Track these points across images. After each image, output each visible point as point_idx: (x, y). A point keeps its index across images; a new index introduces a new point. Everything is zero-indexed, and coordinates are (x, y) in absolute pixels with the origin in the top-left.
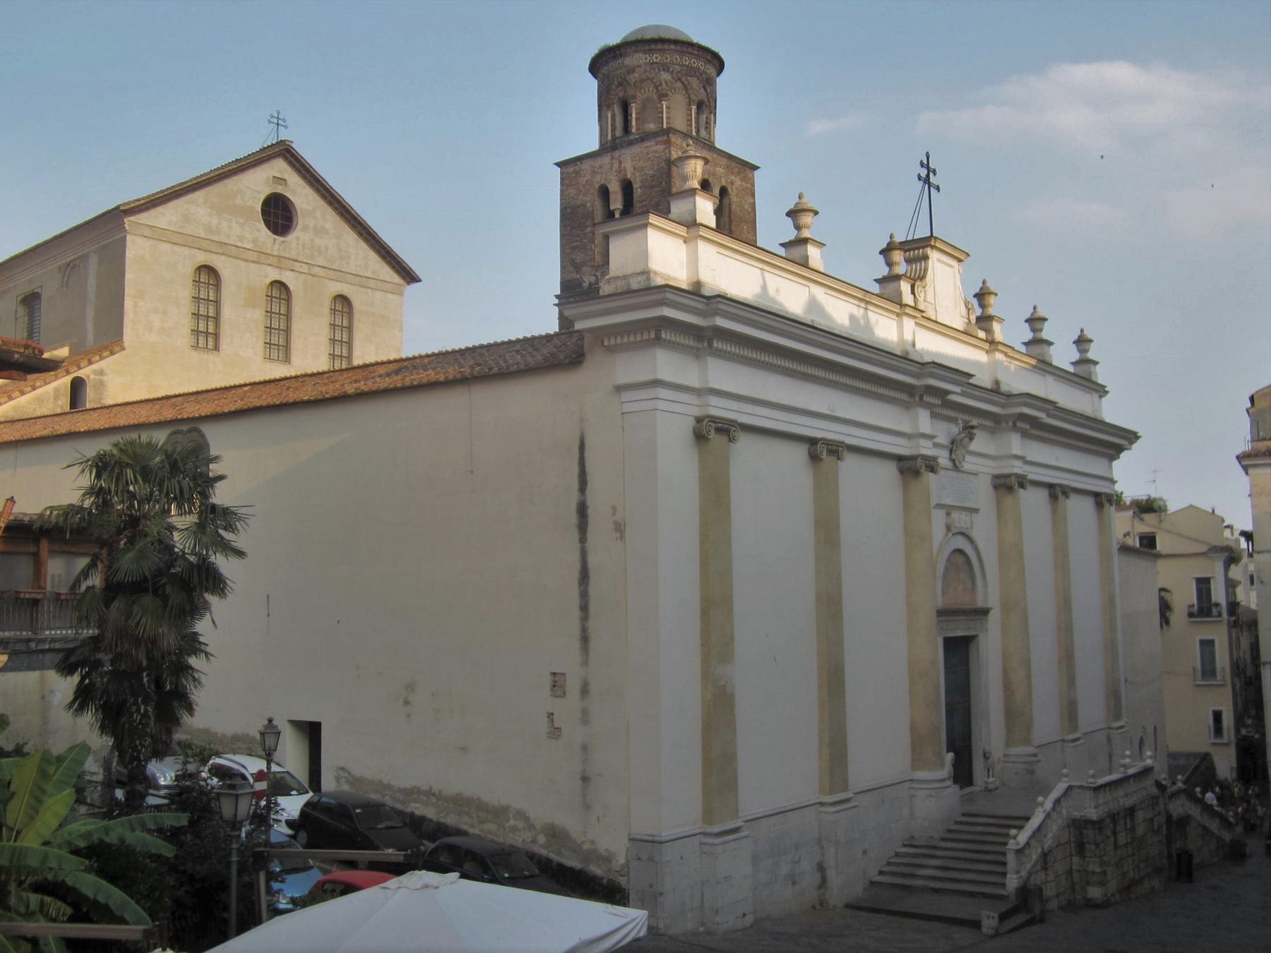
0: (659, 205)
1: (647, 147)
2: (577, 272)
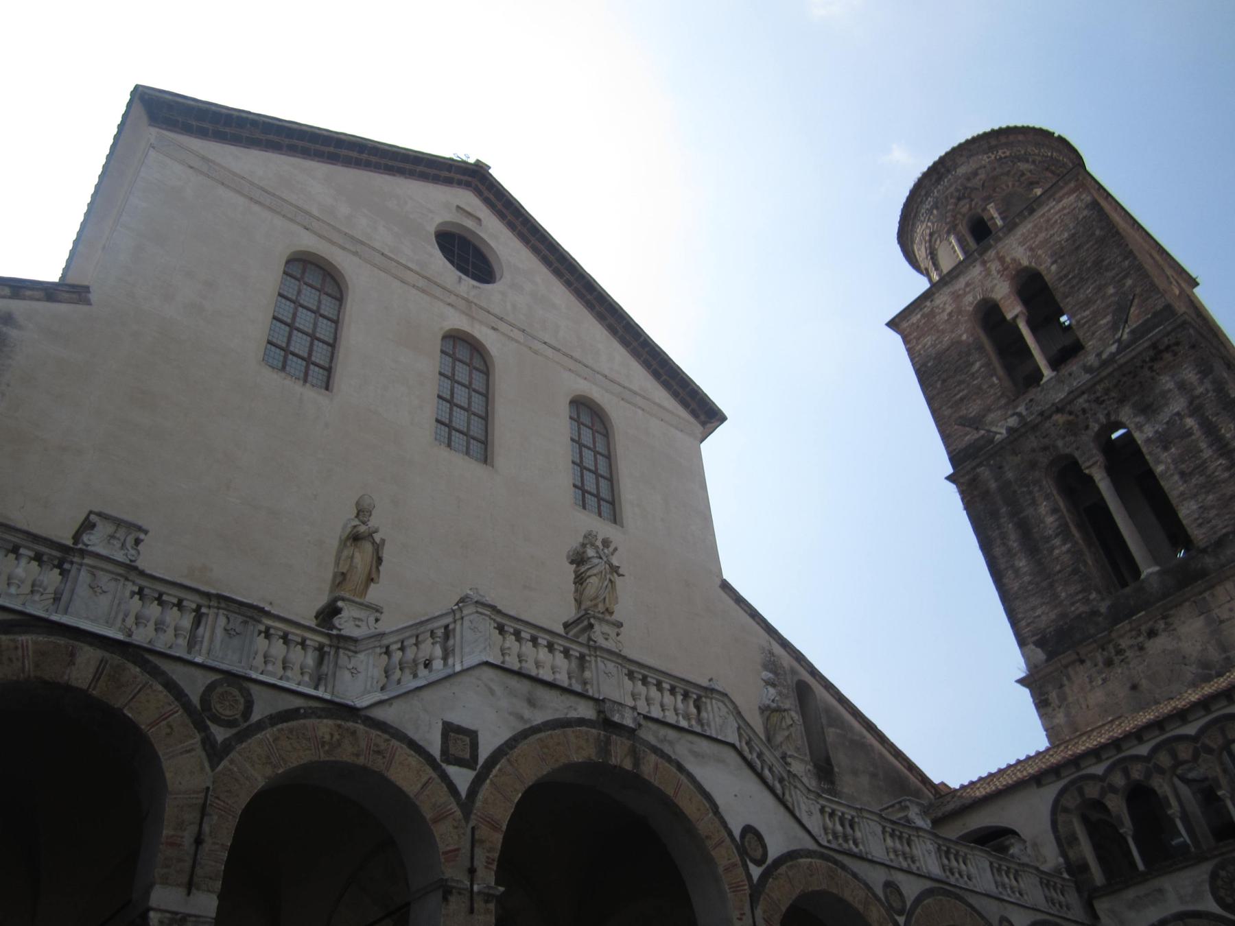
0: (1103, 260)
2: (977, 429)
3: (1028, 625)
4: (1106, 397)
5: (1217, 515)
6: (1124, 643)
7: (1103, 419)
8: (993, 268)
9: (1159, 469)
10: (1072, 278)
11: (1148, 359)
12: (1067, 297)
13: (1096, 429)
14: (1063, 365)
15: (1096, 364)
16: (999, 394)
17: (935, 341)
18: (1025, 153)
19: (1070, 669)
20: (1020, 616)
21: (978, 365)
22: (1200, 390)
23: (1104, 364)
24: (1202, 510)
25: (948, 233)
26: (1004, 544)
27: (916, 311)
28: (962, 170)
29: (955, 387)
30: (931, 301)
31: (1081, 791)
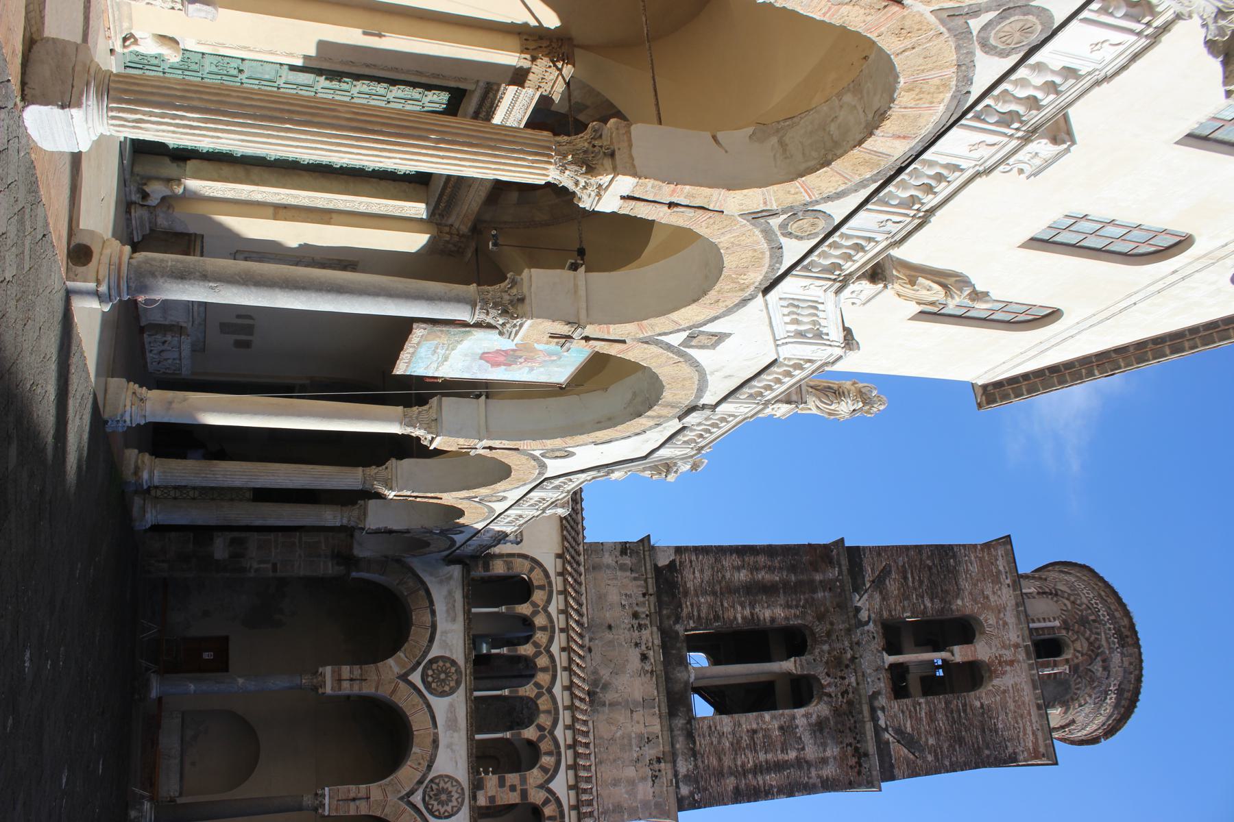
1: (1029, 714)
2: (873, 582)
3: (691, 562)
4: (845, 701)
5: (712, 743)
6: (646, 633)
7: (827, 690)
8: (1007, 652)
9: (767, 716)
10: (960, 714)
11: (859, 745)
12: (946, 703)
13: (823, 681)
14: (889, 676)
15: (876, 704)
16: (893, 613)
17: (970, 575)
18: (1101, 714)
19: (643, 582)
20: (701, 557)
21: (929, 605)
22: (813, 773)
23: (873, 710)
24: (721, 734)
25: (1065, 622)
26: (765, 567)
27: (1007, 568)
28: (1116, 658)
29: (920, 577)
30: (1009, 585)
31: (542, 587)
